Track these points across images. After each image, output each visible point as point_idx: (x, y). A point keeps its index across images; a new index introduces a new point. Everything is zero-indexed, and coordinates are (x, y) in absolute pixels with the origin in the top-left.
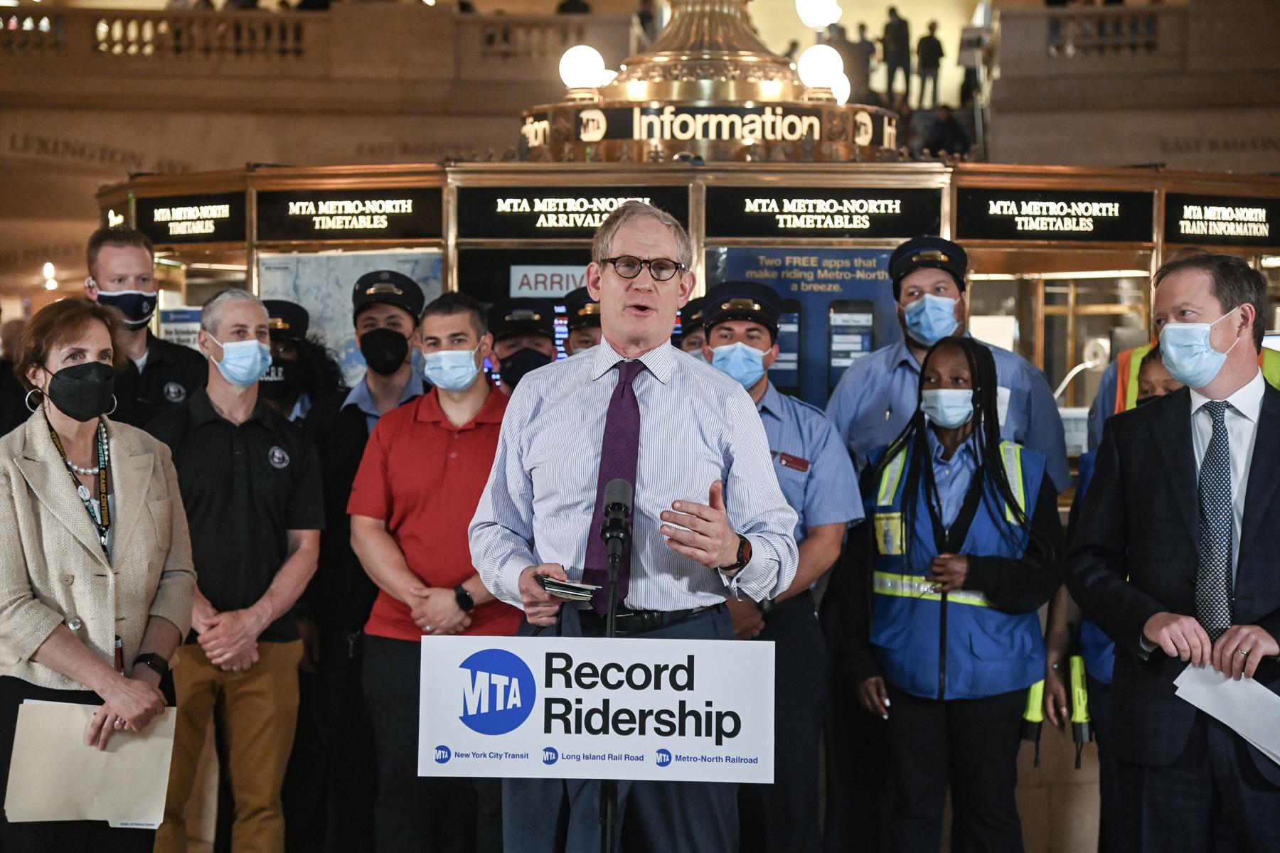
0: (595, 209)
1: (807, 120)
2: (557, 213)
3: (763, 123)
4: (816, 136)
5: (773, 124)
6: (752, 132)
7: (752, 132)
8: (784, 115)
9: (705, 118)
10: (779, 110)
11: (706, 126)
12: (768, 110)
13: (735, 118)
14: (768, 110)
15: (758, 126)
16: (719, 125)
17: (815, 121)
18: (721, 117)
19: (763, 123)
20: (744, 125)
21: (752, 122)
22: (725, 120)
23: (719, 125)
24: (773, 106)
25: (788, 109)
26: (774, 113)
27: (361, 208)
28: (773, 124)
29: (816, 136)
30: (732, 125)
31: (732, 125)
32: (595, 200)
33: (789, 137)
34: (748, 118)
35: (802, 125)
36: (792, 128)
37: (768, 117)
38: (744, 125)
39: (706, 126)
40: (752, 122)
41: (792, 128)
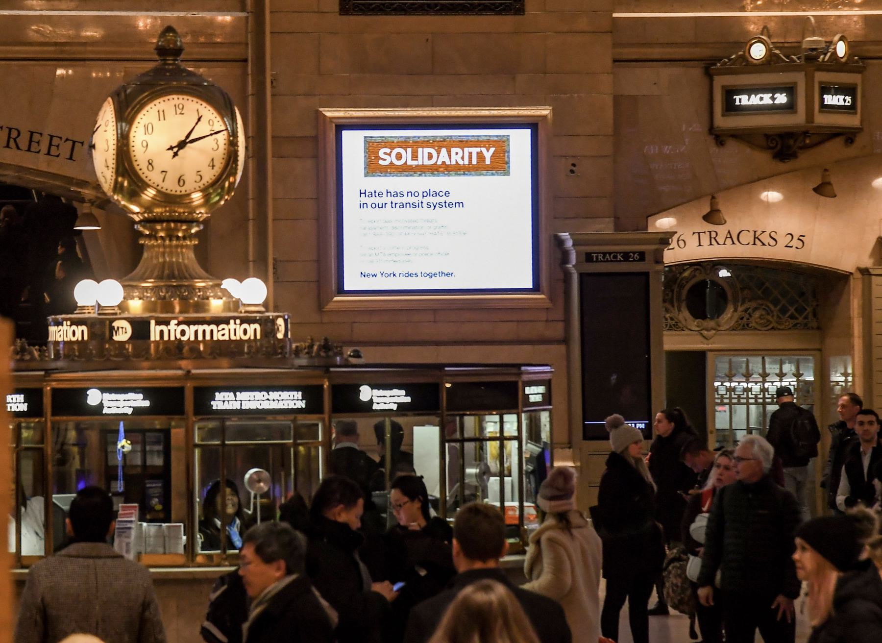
6: (223, 335)
7: (223, 335)
8: (241, 324)
10: (238, 321)
11: (196, 332)
12: (232, 321)
13: (213, 327)
15: (226, 332)
16: (204, 331)
18: (205, 327)
23: (204, 331)
30: (212, 331)
31: (212, 331)
34: (221, 327)
37: (232, 325)
39: (196, 332)
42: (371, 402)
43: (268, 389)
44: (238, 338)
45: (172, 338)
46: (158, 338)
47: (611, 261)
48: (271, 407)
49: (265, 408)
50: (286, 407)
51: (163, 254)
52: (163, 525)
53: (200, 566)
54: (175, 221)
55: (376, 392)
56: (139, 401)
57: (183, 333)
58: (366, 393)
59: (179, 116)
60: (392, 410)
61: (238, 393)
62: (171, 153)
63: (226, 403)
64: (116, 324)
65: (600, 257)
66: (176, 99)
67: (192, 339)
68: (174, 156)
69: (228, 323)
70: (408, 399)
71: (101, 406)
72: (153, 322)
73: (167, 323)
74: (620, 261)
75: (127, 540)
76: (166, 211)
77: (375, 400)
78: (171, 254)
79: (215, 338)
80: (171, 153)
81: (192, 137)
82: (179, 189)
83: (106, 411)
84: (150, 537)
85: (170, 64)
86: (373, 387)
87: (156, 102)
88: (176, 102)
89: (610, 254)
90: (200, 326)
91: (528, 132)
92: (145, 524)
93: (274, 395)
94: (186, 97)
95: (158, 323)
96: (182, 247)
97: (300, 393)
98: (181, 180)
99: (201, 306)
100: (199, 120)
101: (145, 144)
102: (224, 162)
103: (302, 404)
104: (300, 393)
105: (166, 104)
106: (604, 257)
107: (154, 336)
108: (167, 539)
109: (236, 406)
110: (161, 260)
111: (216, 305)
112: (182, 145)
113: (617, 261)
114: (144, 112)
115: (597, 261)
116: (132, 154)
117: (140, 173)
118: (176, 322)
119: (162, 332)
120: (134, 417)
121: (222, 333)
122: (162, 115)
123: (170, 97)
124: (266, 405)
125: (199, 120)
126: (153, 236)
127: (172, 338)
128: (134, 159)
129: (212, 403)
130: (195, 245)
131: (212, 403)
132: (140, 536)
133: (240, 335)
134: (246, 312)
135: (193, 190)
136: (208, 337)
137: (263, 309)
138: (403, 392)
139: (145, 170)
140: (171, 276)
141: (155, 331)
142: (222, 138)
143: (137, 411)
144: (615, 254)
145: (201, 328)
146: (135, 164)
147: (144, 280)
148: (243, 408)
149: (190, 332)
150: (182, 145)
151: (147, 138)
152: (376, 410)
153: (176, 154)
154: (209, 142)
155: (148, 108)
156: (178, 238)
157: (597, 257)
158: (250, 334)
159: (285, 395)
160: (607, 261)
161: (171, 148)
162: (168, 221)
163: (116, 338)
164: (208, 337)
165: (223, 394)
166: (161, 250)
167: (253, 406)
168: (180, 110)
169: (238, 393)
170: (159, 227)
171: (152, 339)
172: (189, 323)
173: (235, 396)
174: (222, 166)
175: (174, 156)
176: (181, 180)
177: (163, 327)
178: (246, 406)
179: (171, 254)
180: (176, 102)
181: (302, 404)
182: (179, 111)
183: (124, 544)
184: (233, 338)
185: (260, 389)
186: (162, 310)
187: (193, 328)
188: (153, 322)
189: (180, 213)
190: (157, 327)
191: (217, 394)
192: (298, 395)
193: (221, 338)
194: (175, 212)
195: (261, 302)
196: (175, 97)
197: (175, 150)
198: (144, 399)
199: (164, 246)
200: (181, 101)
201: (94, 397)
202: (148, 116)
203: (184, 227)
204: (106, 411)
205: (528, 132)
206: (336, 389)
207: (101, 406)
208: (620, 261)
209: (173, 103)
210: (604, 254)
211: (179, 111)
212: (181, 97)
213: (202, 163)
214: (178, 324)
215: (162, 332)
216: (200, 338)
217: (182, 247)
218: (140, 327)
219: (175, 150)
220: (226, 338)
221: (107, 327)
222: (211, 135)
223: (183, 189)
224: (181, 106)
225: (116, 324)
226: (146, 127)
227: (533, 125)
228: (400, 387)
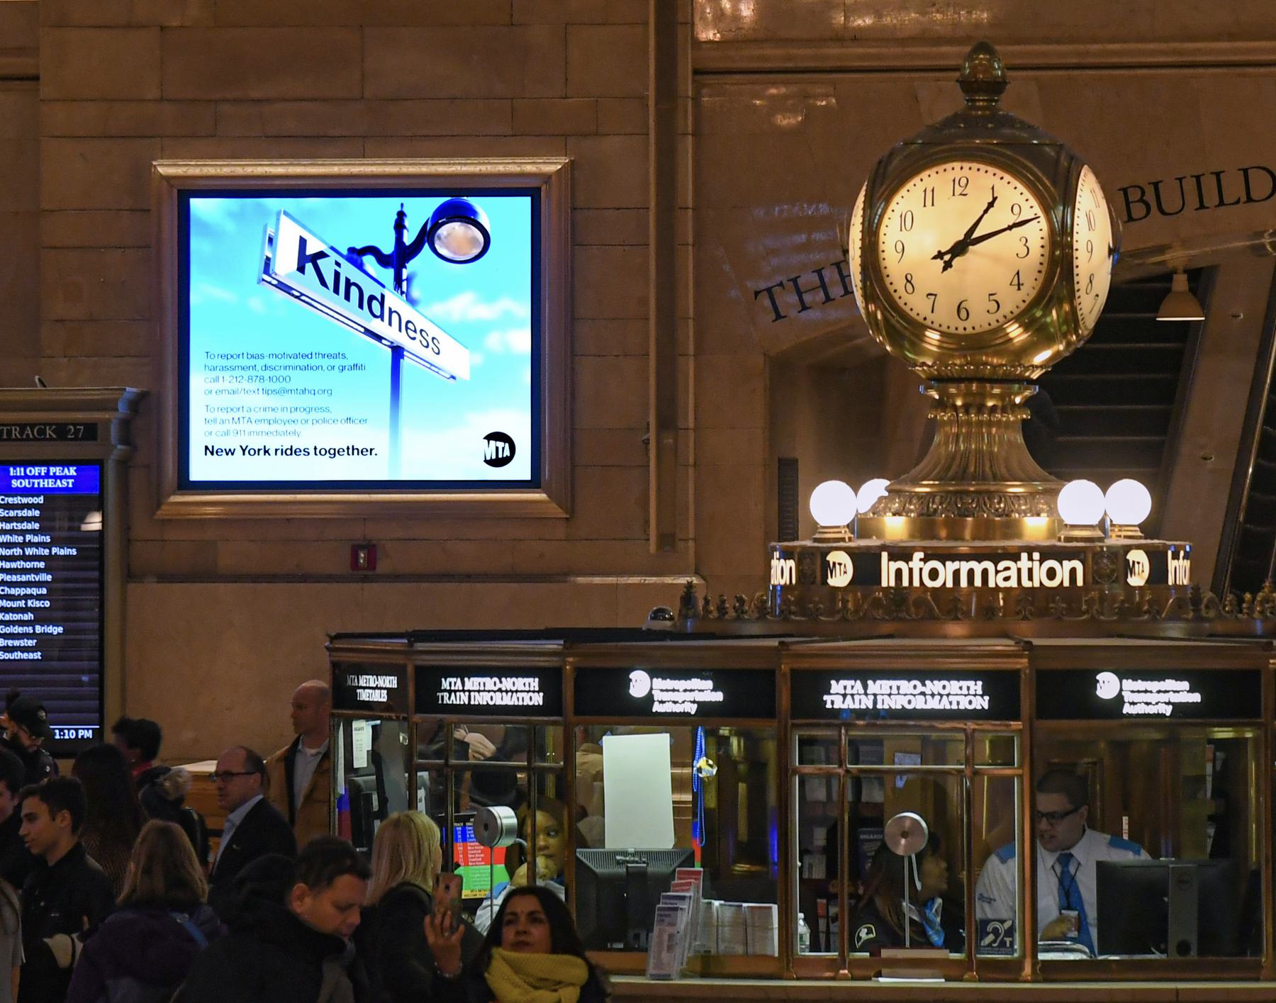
0: (928, 692)
1: (1068, 565)
2: (890, 695)
3: (1019, 570)
4: (1080, 582)
5: (1030, 571)
6: (1007, 579)
7: (1007, 579)
8: (1041, 562)
9: (956, 565)
10: (1036, 556)
11: (957, 574)
12: (1024, 556)
13: (988, 565)
14: (1024, 556)
15: (1013, 573)
16: (971, 573)
17: (1077, 565)
18: (973, 564)
19: (1019, 570)
20: (997, 572)
21: (1007, 569)
22: (978, 567)
23: (971, 573)
24: (1030, 550)
25: (1047, 553)
26: (1030, 559)
27: (499, 685)
28: (1030, 571)
29: (1080, 582)
30: (985, 573)
31: (985, 573)
32: (928, 682)
33: (1048, 583)
34: (1001, 565)
35: (1063, 571)
36: (1051, 574)
37: (1024, 563)
38: (997, 572)
39: (957, 574)
40: (1007, 569)
41: (1051, 574)
42: (649, 698)
43: (923, 675)
44: (1037, 584)
45: (916, 583)
46: (892, 584)
47: (35, 439)
48: (928, 707)
49: (918, 707)
50: (954, 707)
51: (957, 436)
52: (745, 905)
53: (1026, 981)
54: (982, 380)
55: (659, 683)
56: (1181, 692)
57: (934, 574)
58: (1107, 685)
59: (957, 198)
60: (1163, 716)
61: (870, 682)
62: (940, 263)
63: (849, 697)
64: (832, 557)
65: (15, 433)
66: (956, 170)
67: (950, 584)
68: (945, 269)
69: (1016, 558)
70: (719, 697)
71: (1119, 700)
72: (885, 555)
73: (907, 558)
74: (51, 439)
75: (670, 930)
76: (968, 363)
77: (657, 695)
78: (968, 437)
79: (991, 584)
80: (940, 263)
81: (976, 235)
82: (961, 325)
83: (1127, 709)
84: (723, 926)
85: (980, 108)
86: (653, 674)
87: (924, 175)
88: (957, 173)
89: (32, 426)
90: (963, 563)
91: (526, 202)
92: (716, 903)
93: (935, 686)
94: (975, 166)
95: (892, 558)
96: (999, 423)
97: (979, 683)
98: (961, 310)
99: (1011, 529)
100: (991, 205)
101: (899, 247)
102: (1041, 277)
103: (982, 703)
104: (979, 683)
105: (935, 179)
106: (21, 433)
107: (887, 580)
108: (749, 930)
109: (867, 703)
110: (952, 448)
111: (1035, 527)
112: (959, 249)
113: (45, 439)
114: (903, 192)
115: (9, 439)
116: (883, 264)
117: (896, 296)
118: (920, 555)
119: (899, 572)
120: (1174, 720)
121: (1004, 576)
122: (930, 198)
123: (949, 166)
124: (919, 703)
125: (991, 205)
126: (941, 405)
127: (916, 583)
128: (885, 272)
129: (825, 697)
130: (1024, 421)
131: (825, 697)
132: (706, 923)
133: (1040, 575)
134: (1068, 539)
135: (936, 326)
136: (978, 582)
137: (1099, 534)
138: (1185, 685)
139: (901, 292)
140: (962, 476)
141: (888, 570)
142: (1037, 233)
143: (1180, 709)
144: (41, 427)
145: (965, 566)
146: (887, 281)
147: (916, 482)
148: (879, 706)
149: (946, 572)
150: (959, 249)
151: (904, 236)
152: (1130, 716)
153: (948, 265)
154: (1009, 244)
155: (910, 185)
156: (955, 408)
157: (9, 432)
158: (1063, 576)
159: (953, 686)
160: (28, 439)
161: (940, 255)
162: (970, 380)
163: (832, 582)
164: (978, 582)
165: (843, 683)
166: (955, 430)
167: (897, 703)
168: (960, 188)
169: (870, 682)
170: (953, 390)
171: (884, 584)
172: (944, 557)
173: (865, 687)
174: (1038, 285)
175: (945, 269)
176: (961, 310)
177: (901, 564)
178: (885, 703)
179: (968, 437)
180: (957, 173)
181: (982, 703)
182: (958, 190)
183: (666, 937)
184: (1026, 583)
185: (908, 675)
186: (934, 535)
187: (952, 566)
188: (885, 555)
189: (994, 367)
190: (892, 563)
191: (833, 682)
192: (977, 686)
193: (1002, 584)
194: (986, 364)
195: (1095, 522)
196: (957, 165)
197: (947, 257)
198: (1191, 691)
199: (959, 426)
200: (966, 172)
201: (1107, 685)
202: (907, 199)
203: (996, 391)
204: (1127, 709)
205: (526, 202)
206: (1045, 679)
207: (1119, 700)
208: (51, 439)
209: (950, 175)
210: (23, 427)
211: (958, 190)
212: (966, 165)
213: (1000, 280)
214: (925, 560)
215: (899, 572)
216: (964, 583)
217: (990, 424)
218: (866, 564)
219: (947, 257)
220: (1013, 583)
221: (819, 562)
222: (1010, 228)
223: (968, 324)
224: (964, 181)
225: (832, 557)
226: (903, 218)
227: (531, 189)
228: (1178, 676)
